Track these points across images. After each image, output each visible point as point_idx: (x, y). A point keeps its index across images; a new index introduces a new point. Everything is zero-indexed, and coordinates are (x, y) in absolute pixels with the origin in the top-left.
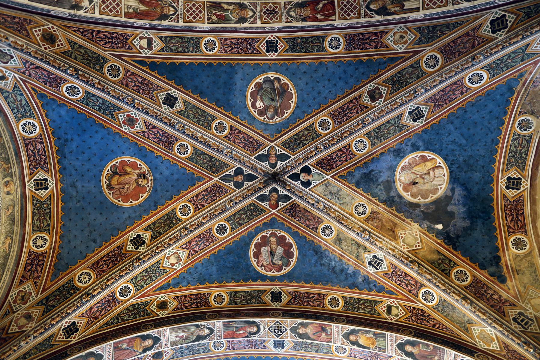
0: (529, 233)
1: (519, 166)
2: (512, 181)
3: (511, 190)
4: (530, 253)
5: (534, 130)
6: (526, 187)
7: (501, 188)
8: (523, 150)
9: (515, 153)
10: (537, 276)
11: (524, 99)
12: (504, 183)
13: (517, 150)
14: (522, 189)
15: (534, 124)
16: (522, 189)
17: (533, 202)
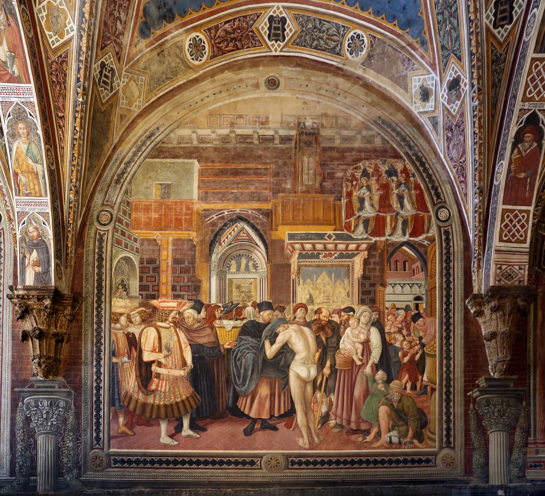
0: (215, 61)
1: (301, 36)
2: (280, 25)
3: (268, 25)
4: (189, 67)
5: (347, 59)
6: (273, 49)
7: (269, 7)
8: (322, 42)
9: (319, 29)
10: (164, 82)
11: (391, 43)
12: (278, 13)
13: (323, 32)
14: (270, 43)
15: (356, 59)
16: (270, 43)
17: (255, 63)
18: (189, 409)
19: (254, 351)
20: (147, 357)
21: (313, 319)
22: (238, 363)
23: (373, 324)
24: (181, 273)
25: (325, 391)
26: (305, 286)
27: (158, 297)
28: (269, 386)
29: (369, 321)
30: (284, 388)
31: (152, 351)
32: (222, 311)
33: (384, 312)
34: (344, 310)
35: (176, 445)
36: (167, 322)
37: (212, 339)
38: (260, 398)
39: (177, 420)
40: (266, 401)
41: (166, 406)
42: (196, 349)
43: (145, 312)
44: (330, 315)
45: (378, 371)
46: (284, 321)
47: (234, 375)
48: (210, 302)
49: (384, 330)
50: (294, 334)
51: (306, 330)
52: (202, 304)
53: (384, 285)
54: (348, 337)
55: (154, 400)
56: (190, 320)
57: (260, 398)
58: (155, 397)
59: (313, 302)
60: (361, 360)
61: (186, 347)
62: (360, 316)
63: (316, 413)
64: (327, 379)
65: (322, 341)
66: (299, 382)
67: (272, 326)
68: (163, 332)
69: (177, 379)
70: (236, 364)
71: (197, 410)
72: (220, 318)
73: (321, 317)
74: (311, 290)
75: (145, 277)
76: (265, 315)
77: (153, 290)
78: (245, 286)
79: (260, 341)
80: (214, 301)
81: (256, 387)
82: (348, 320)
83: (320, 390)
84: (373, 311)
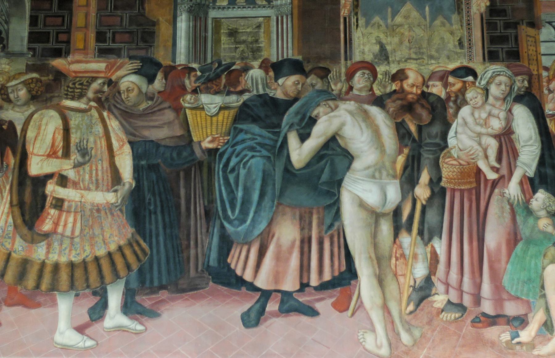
18: (122, 271)
19: (265, 153)
20: (36, 168)
21: (388, 90)
22: (231, 177)
23: (519, 99)
24: (116, 8)
25: (421, 233)
26: (369, 29)
27: (68, 53)
28: (297, 222)
29: (510, 94)
30: (331, 226)
31: (49, 156)
32: (198, 78)
33: (539, 76)
34: (455, 72)
35: (91, 348)
36: (85, 100)
37: (179, 132)
38: (279, 246)
39: (95, 293)
40: (290, 252)
41: (72, 265)
42: (142, 151)
43: (38, 80)
44: (425, 83)
45: (534, 192)
46: (329, 96)
47: (222, 201)
48: (174, 60)
49: (542, 110)
50: (348, 118)
51: (374, 110)
52: (158, 65)
53: (534, 24)
54: (466, 123)
55: (48, 253)
56: (133, 95)
57: (279, 246)
58: (49, 246)
59: (387, 58)
60: (496, 170)
61: (121, 147)
62: (488, 83)
63: (401, 279)
64: (424, 208)
65: (409, 133)
66: (363, 214)
67: (303, 106)
68: (75, 120)
69: (98, 211)
70: (226, 179)
71: (141, 271)
72: (195, 91)
73: (405, 86)
74: (382, 36)
75: (41, 16)
76: (289, 84)
77: (57, 41)
78: (245, 29)
79: (278, 134)
80: (181, 59)
81: (270, 224)
82: (463, 91)
83: (409, 230)
84: (516, 75)
